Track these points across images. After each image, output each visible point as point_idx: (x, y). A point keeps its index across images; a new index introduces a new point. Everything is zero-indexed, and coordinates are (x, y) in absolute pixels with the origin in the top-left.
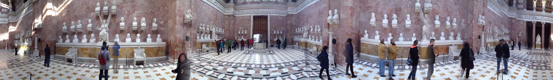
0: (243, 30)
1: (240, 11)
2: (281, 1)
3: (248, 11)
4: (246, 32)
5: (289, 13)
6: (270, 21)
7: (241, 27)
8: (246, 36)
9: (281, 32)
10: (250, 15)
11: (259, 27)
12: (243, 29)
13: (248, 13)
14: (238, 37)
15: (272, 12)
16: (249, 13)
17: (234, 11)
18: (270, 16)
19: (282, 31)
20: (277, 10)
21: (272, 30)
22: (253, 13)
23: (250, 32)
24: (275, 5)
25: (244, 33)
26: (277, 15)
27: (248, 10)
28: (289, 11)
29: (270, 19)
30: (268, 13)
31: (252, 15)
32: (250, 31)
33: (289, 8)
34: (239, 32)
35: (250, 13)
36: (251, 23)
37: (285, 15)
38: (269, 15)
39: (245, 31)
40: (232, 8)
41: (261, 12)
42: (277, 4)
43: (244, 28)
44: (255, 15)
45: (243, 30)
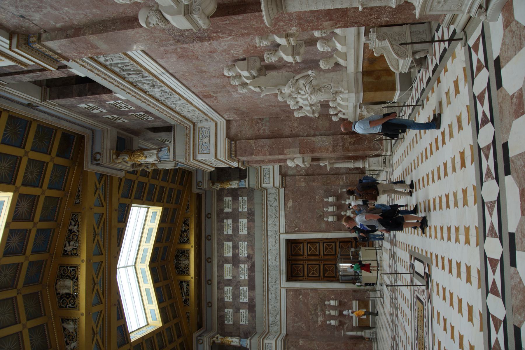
0: (327, 313)
1: (270, 318)
2: (246, 203)
3: (273, 295)
4: (332, 303)
5: (277, 183)
6: (299, 231)
7: (317, 316)
8: (345, 303)
9: (331, 199)
10: (283, 292)
11: (317, 262)
12: (323, 311)
13: (278, 298)
14: (346, 326)
15: (277, 228)
16: (278, 294)
17: (271, 337)
18: (286, 232)
19: (328, 198)
20: (269, 213)
21: (324, 225)
22: (278, 282)
23: (333, 291)
24: (257, 218)
25: (334, 308)
26: (282, 213)
27: (272, 296)
28: (272, 184)
29: (295, 232)
30: (278, 237)
31: (285, 284)
32: (328, 290)
33: (264, 185)
34: (333, 322)
35: (278, 291)
36: (305, 289)
37: (282, 190)
38: (285, 237)
39: (329, 305)
40: (266, 341)
41: (278, 260)
42: (254, 215)
43: (319, 309)
44: (284, 277)
45: (327, 313)
